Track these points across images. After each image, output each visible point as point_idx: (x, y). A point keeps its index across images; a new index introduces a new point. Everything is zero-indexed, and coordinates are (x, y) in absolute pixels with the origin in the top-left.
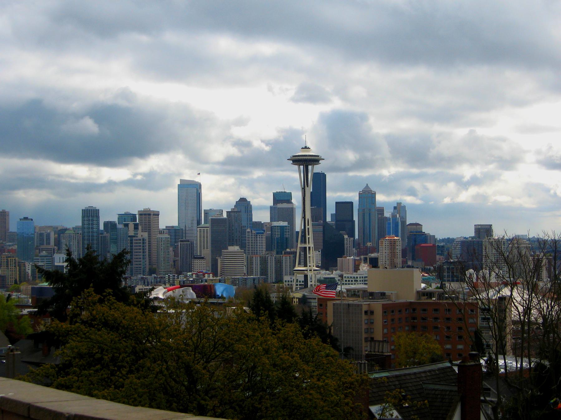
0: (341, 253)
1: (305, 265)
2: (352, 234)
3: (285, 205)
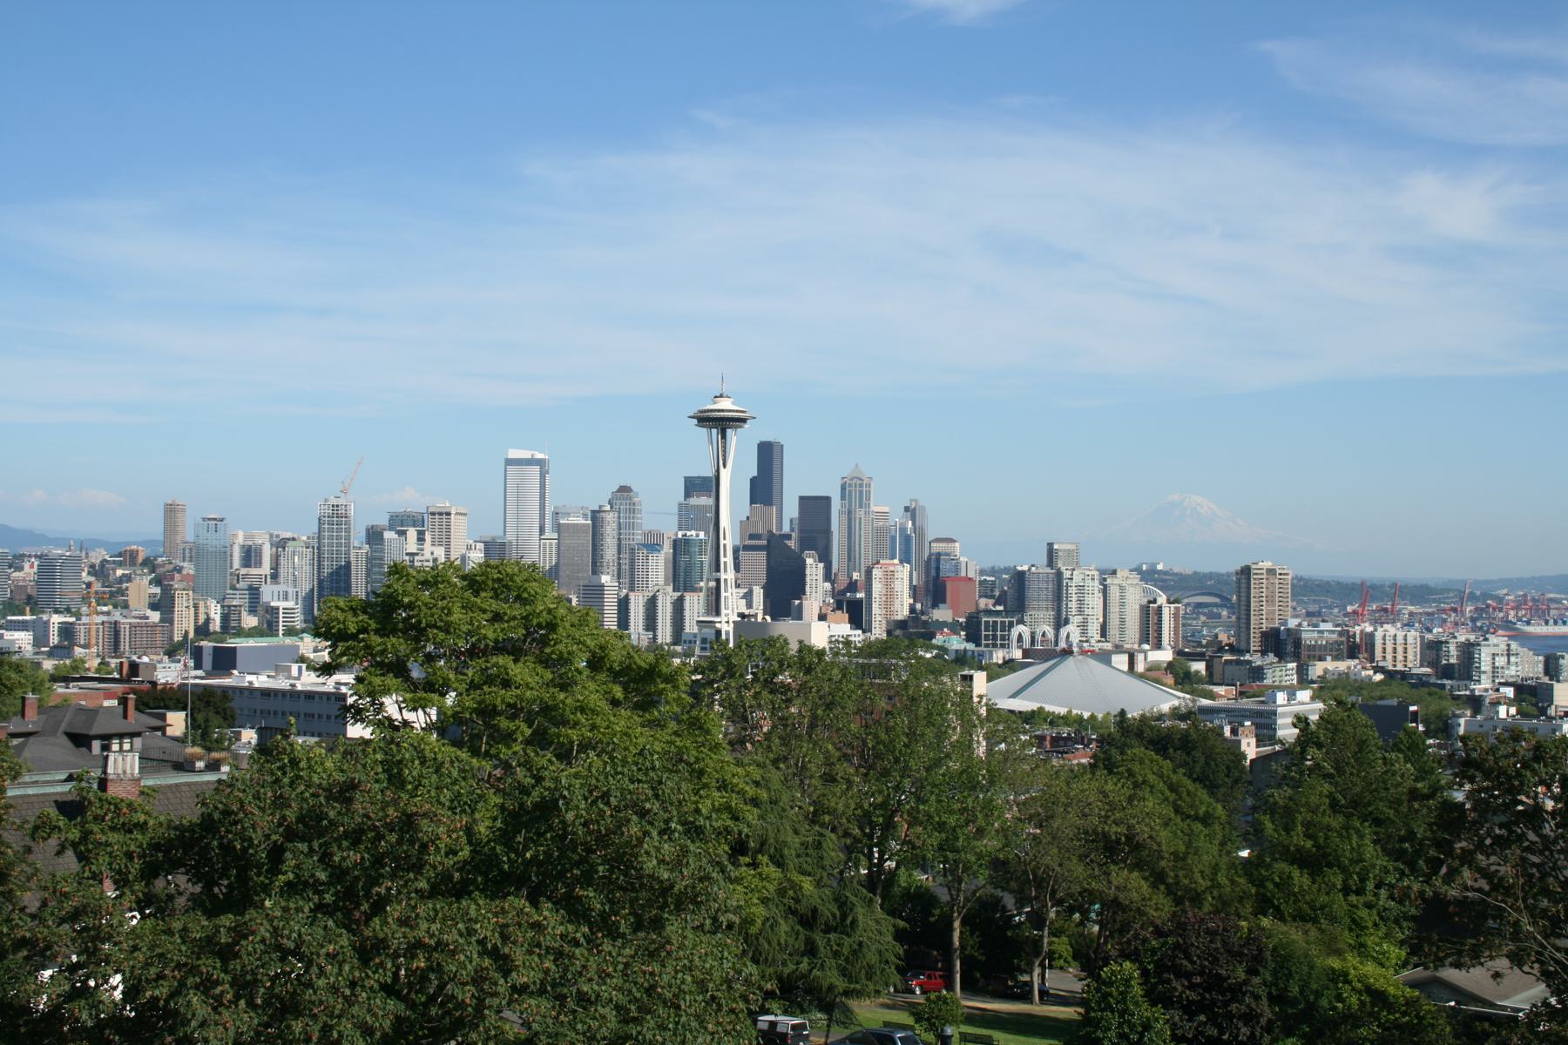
0: (799, 590)
1: (718, 613)
2: (825, 558)
3: (706, 501)
